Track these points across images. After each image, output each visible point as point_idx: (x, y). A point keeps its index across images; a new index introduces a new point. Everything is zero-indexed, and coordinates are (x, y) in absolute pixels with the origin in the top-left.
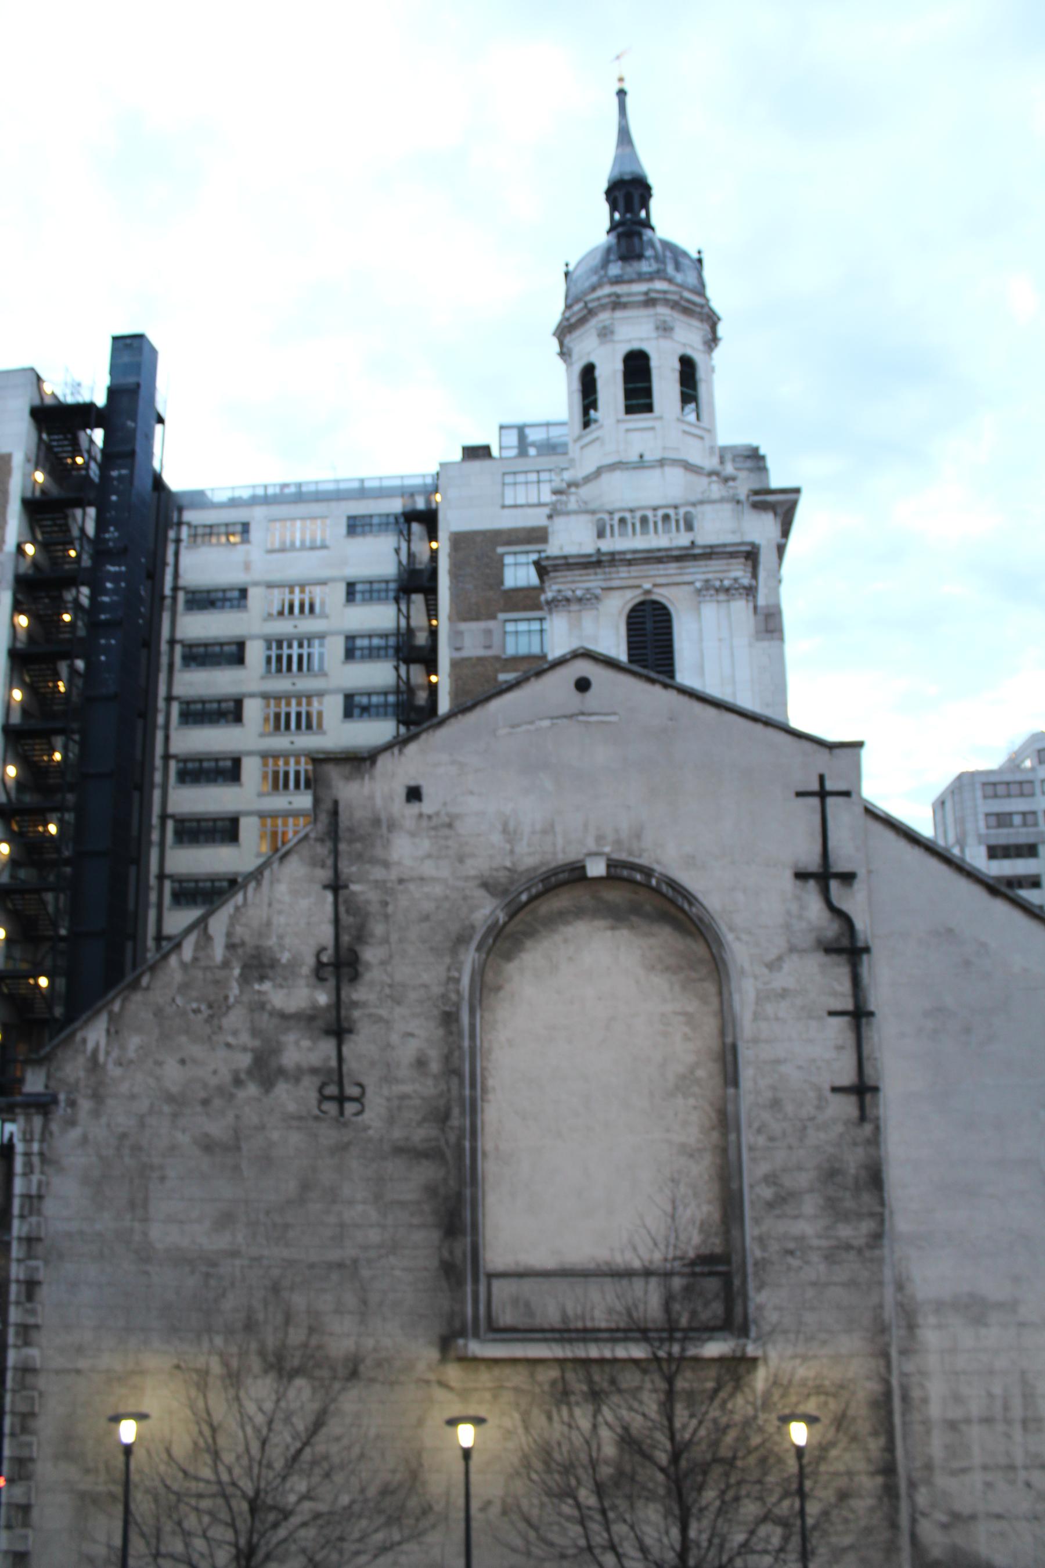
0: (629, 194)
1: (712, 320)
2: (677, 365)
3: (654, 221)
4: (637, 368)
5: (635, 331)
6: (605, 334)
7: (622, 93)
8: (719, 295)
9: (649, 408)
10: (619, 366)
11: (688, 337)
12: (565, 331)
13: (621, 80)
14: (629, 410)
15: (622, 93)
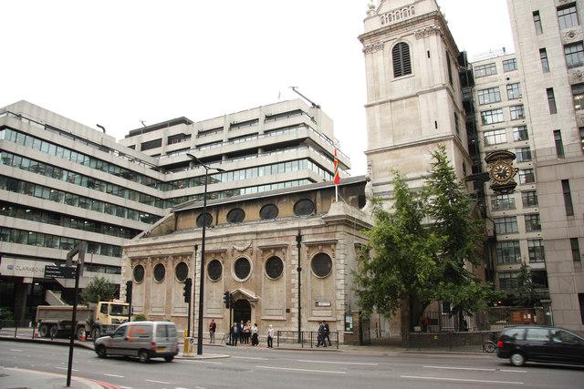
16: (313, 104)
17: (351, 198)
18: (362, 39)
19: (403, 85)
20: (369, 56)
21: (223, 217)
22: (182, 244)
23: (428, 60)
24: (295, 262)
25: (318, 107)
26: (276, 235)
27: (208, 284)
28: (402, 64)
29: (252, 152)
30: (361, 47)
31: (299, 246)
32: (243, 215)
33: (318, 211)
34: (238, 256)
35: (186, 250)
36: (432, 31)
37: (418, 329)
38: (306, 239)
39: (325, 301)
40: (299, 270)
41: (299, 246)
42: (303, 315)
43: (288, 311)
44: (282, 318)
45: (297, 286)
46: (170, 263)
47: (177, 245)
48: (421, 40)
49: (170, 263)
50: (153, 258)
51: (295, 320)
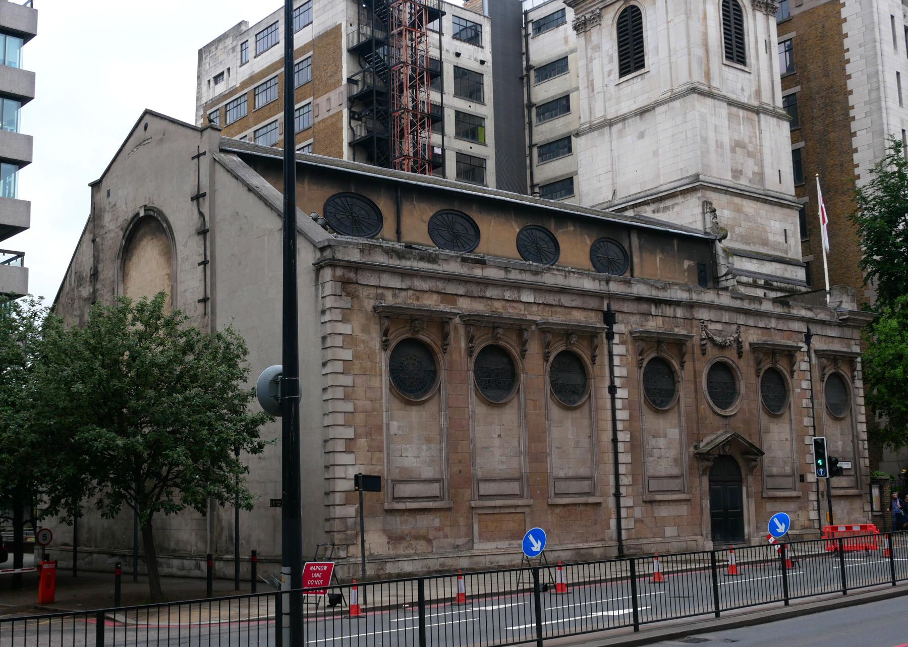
17: (686, 264)
22: (566, 300)
24: (805, 385)
26: (773, 324)
27: (651, 421)
33: (637, 272)
34: (713, 354)
35: (579, 317)
38: (818, 344)
41: (808, 352)
43: (802, 478)
44: (794, 494)
46: (534, 348)
47: (550, 299)
49: (534, 348)
50: (471, 321)
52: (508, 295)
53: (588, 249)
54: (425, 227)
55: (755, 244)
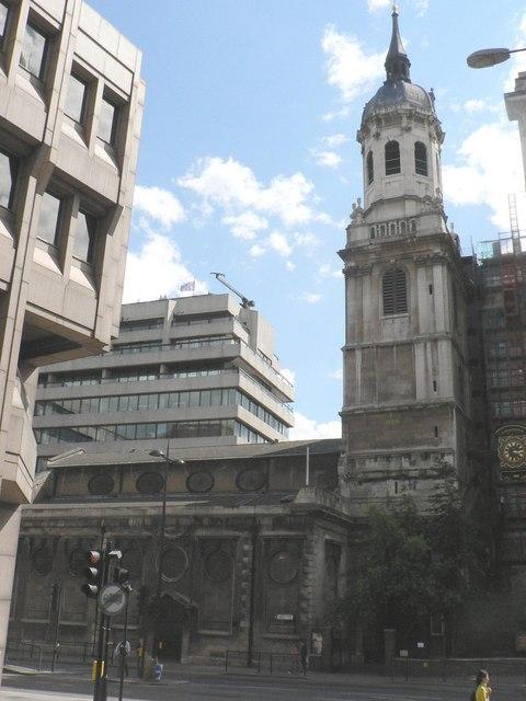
0: (397, 66)
1: (434, 122)
2: (414, 147)
3: (411, 77)
4: (392, 151)
5: (390, 134)
6: (377, 136)
7: (395, 16)
8: (439, 110)
9: (398, 171)
10: (383, 151)
11: (420, 133)
12: (363, 134)
13: (394, 9)
14: (388, 173)
15: (395, 16)
16: (244, 300)
18: (342, 254)
19: (394, 330)
20: (352, 282)
21: (130, 484)
23: (431, 296)
25: (251, 304)
28: (396, 298)
29: (151, 369)
30: (341, 264)
31: (254, 540)
32: (164, 483)
35: (86, 532)
36: (437, 260)
37: (404, 653)
39: (287, 612)
40: (253, 570)
42: (256, 630)
45: (248, 592)
48: (422, 272)
51: (244, 636)
52: (52, 524)
53: (234, 478)
54: (134, 484)
55: (397, 446)
